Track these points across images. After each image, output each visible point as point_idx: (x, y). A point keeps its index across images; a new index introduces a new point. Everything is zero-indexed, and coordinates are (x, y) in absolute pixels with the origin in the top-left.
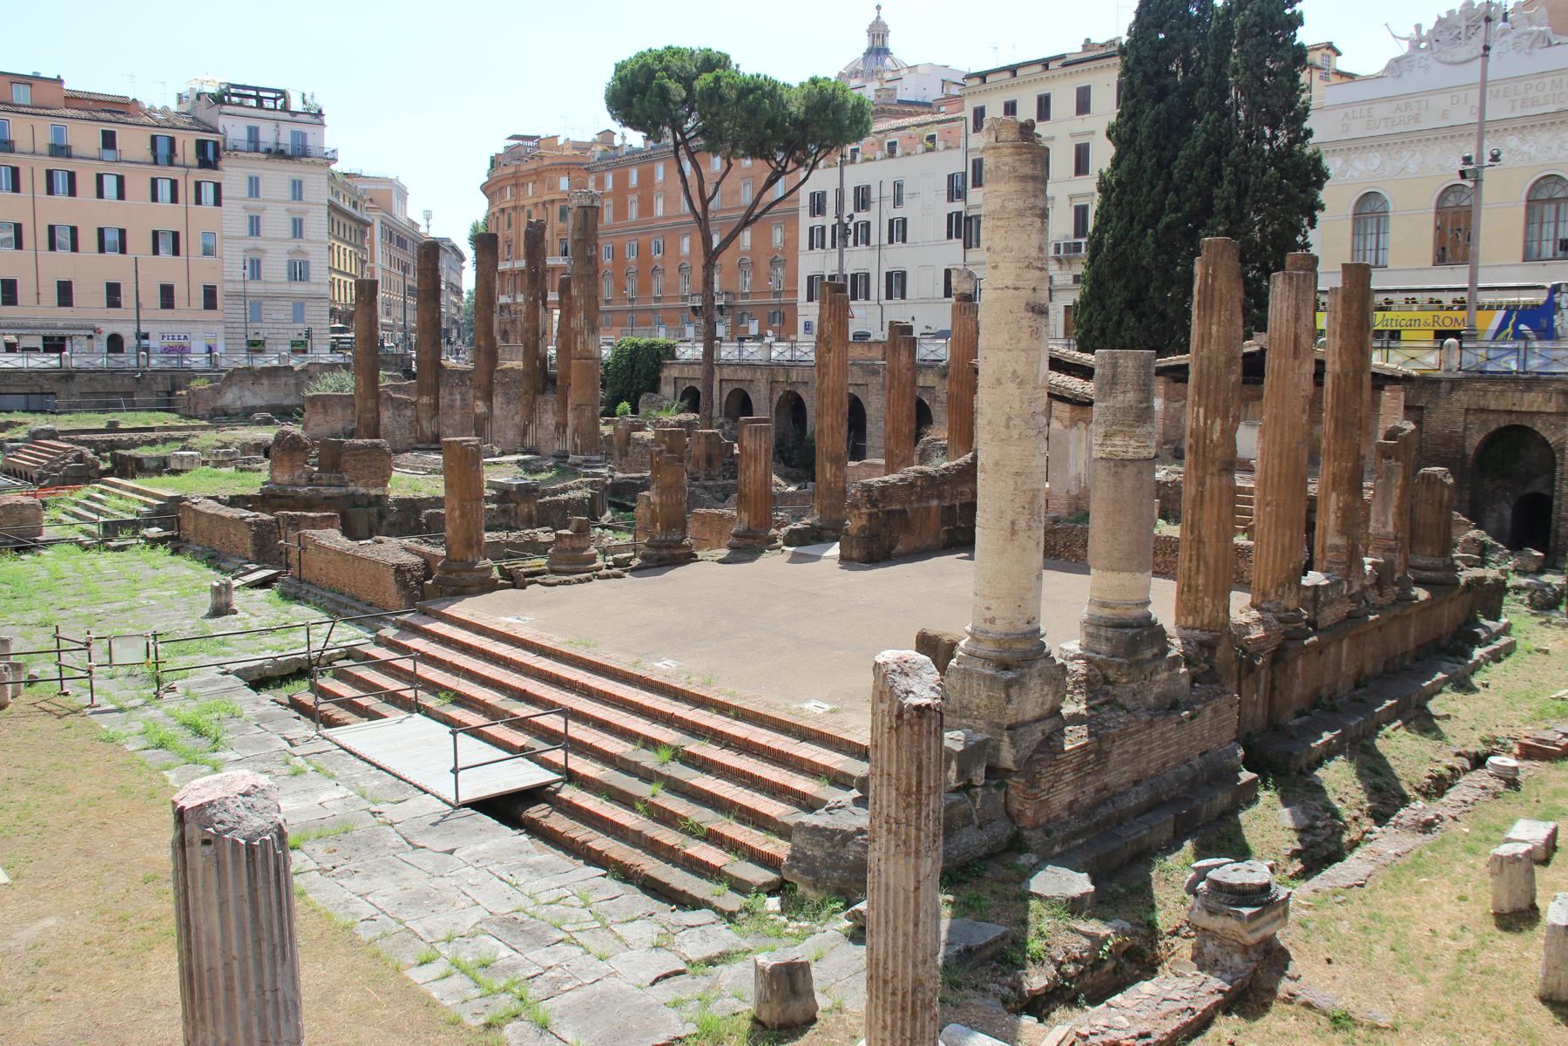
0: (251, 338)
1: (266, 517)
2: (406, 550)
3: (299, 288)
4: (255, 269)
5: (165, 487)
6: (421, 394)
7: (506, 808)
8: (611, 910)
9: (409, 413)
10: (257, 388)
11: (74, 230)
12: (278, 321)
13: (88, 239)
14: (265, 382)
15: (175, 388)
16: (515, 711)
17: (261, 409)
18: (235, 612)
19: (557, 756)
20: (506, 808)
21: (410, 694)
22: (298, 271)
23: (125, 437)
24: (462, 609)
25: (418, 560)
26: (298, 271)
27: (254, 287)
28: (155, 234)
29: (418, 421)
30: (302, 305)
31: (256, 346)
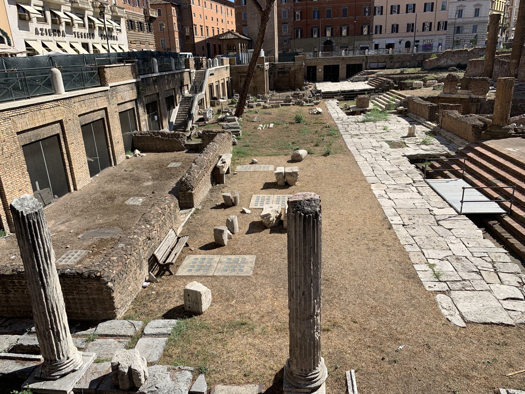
0: (455, 39)
1: (435, 105)
2: (480, 120)
3: (476, 19)
4: (460, 13)
5: (407, 93)
6: (513, 59)
7: (480, 220)
8: (502, 267)
9: (506, 66)
10: (453, 58)
11: (399, 6)
12: (466, 33)
13: (403, 9)
14: (456, 56)
15: (424, 59)
16: (498, 184)
17: (454, 66)
18: (415, 136)
19: (508, 204)
20: (480, 220)
21: (461, 172)
22: (477, 12)
23: (404, 76)
24: (491, 143)
25: (482, 123)
26: (477, 12)
27: (459, 20)
28: (425, 4)
29: (509, 69)
30: (477, 26)
31: (457, 43)
